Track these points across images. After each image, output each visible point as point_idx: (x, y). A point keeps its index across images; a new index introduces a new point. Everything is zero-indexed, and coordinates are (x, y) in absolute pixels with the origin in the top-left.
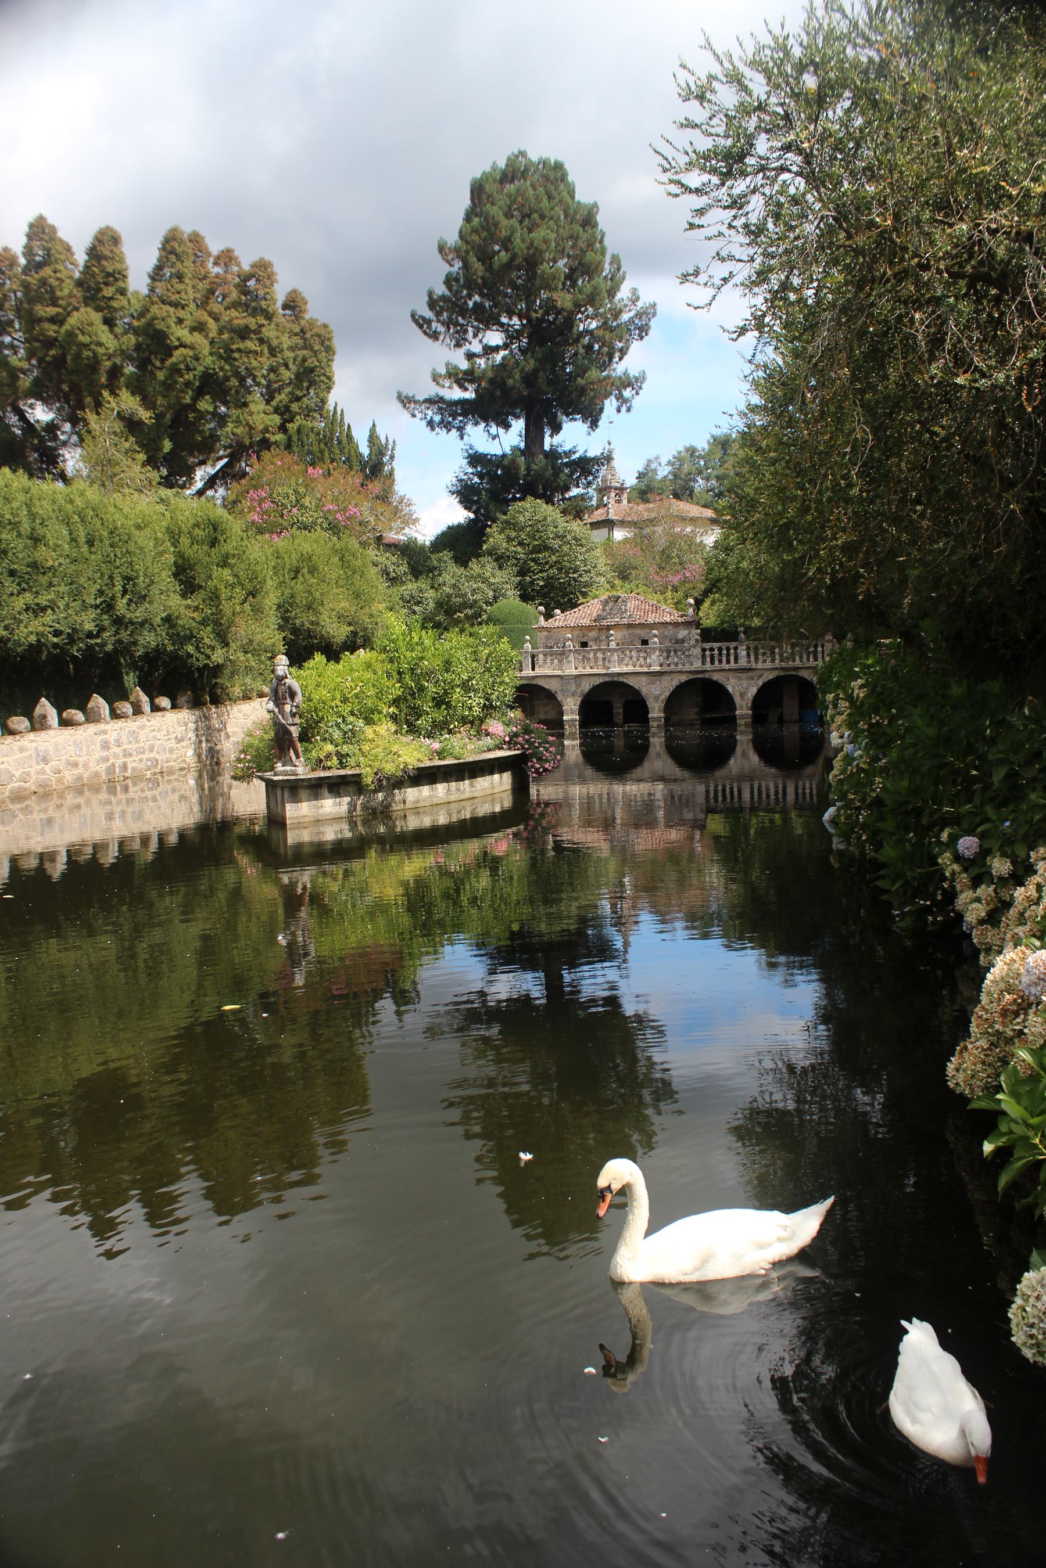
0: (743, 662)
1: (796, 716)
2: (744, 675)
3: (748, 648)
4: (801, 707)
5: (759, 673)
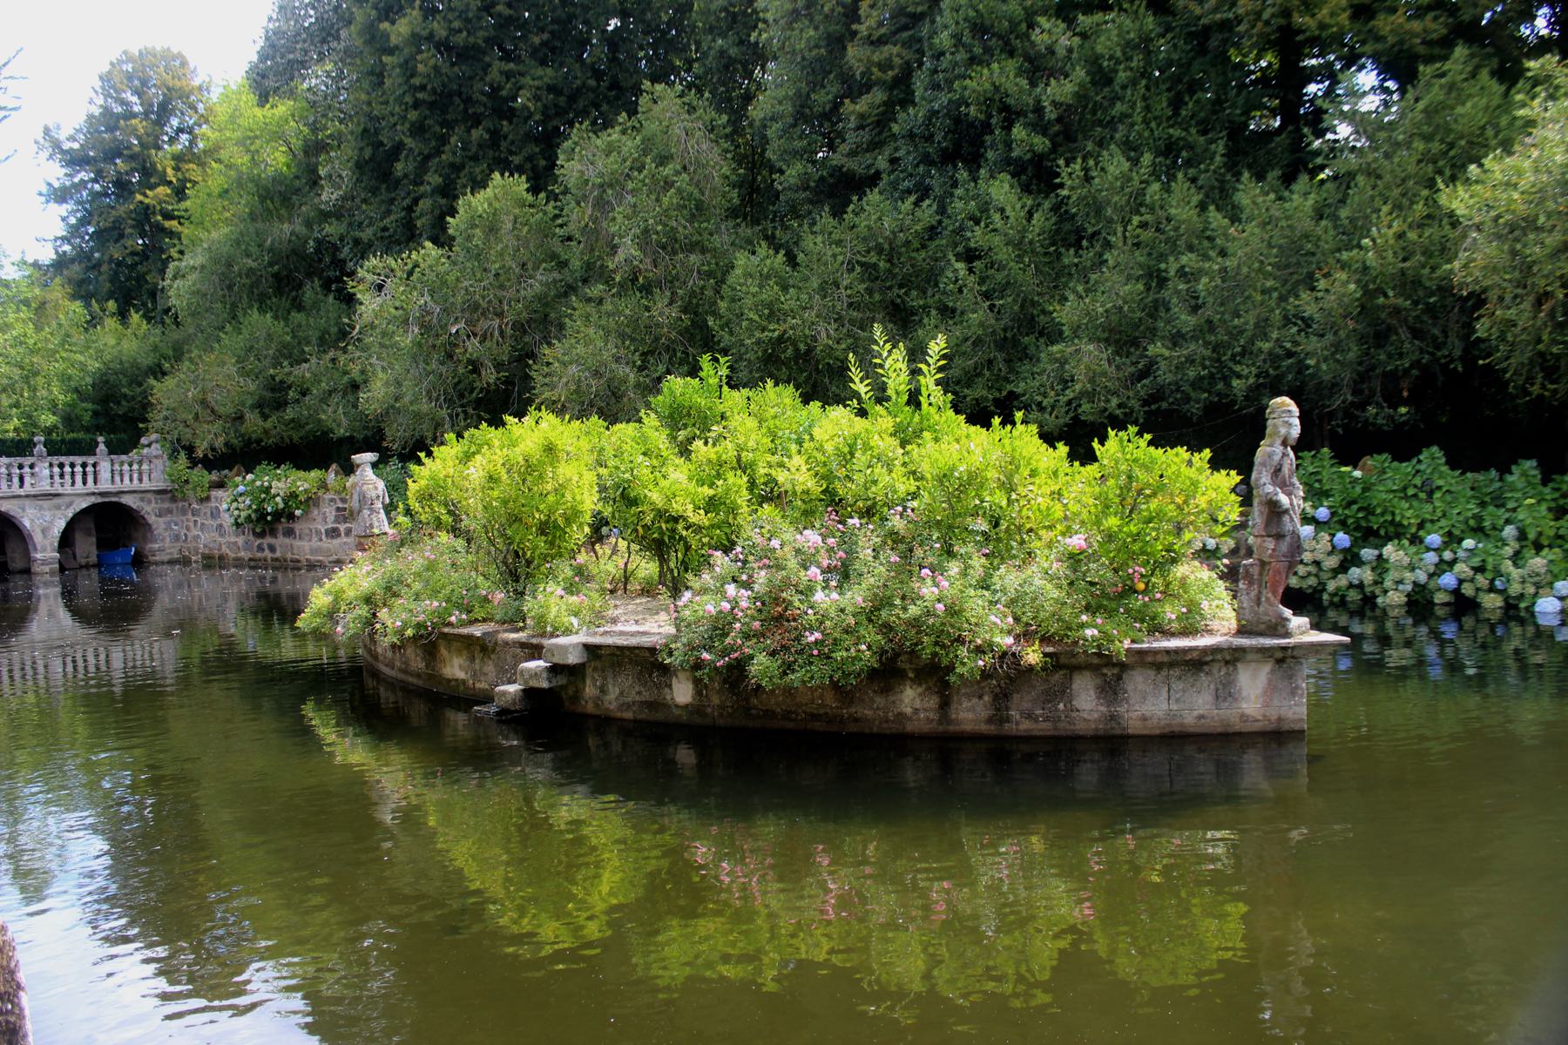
0: (45, 486)
1: (93, 559)
2: (46, 504)
3: (51, 465)
4: (99, 547)
5: (67, 499)
